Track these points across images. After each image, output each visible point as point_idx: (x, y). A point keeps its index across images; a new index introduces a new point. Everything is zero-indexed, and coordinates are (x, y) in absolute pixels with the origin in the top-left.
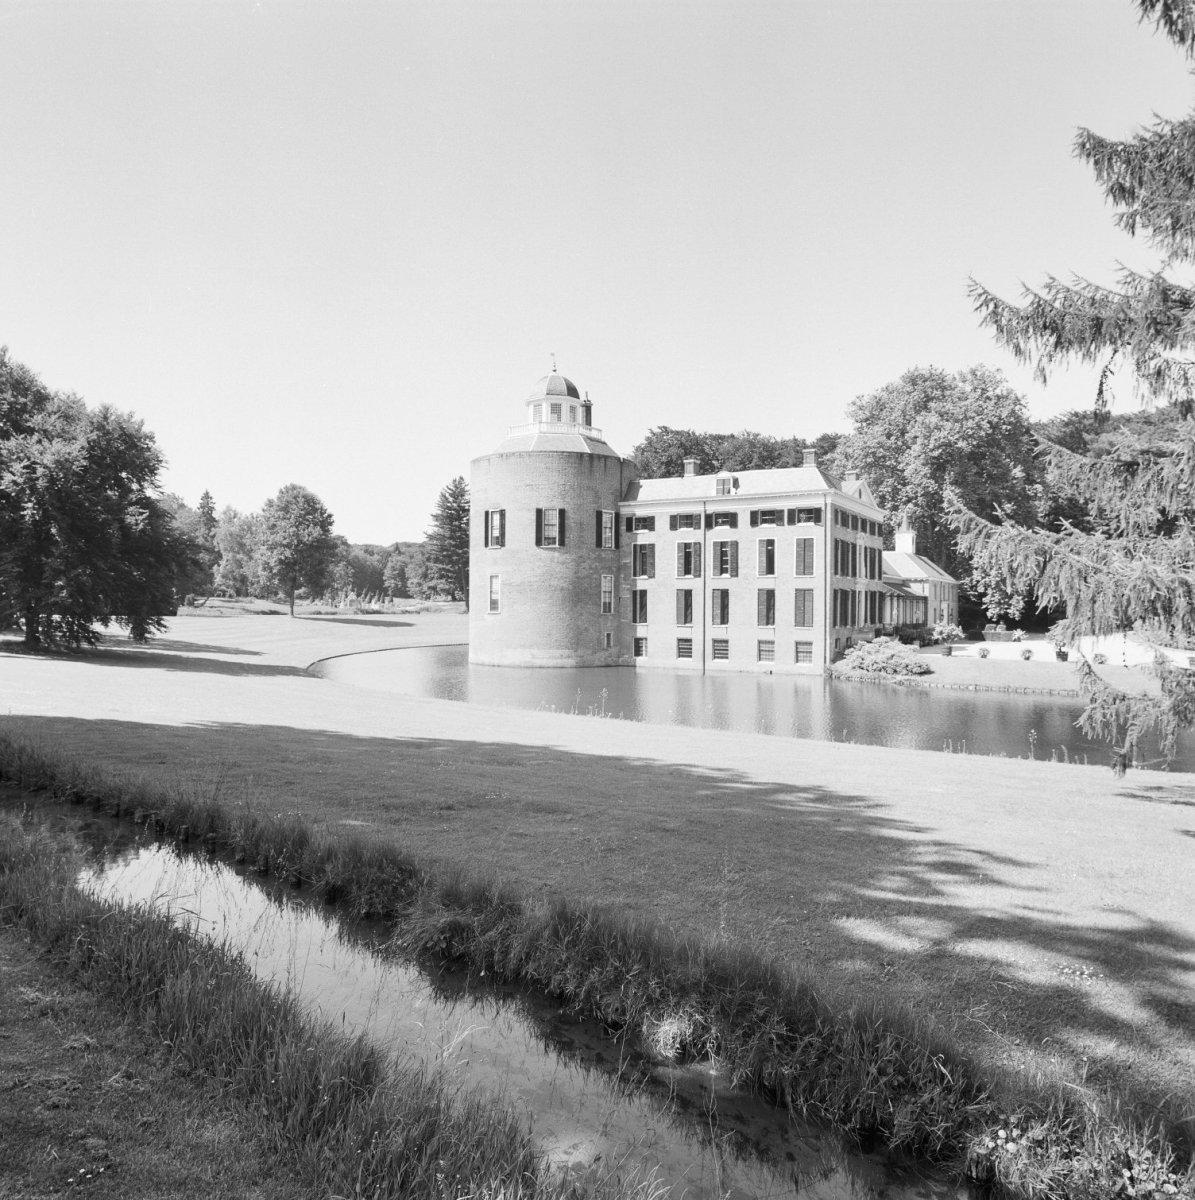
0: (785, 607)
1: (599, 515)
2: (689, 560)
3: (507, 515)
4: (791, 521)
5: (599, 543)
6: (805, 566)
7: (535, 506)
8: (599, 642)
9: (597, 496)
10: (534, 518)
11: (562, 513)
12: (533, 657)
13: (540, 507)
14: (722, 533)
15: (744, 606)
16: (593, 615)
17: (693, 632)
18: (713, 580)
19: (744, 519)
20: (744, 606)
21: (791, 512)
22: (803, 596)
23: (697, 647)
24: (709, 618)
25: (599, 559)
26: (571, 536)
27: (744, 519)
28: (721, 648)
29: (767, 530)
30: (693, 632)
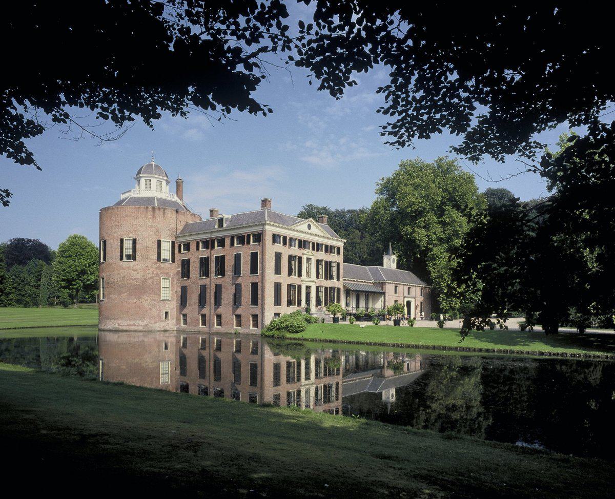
1: (159, 243)
5: (159, 258)
7: (120, 237)
8: (159, 316)
9: (157, 231)
11: (134, 241)
12: (119, 325)
14: (218, 251)
15: (228, 295)
16: (155, 300)
17: (205, 311)
20: (228, 295)
25: (159, 268)
26: (138, 253)
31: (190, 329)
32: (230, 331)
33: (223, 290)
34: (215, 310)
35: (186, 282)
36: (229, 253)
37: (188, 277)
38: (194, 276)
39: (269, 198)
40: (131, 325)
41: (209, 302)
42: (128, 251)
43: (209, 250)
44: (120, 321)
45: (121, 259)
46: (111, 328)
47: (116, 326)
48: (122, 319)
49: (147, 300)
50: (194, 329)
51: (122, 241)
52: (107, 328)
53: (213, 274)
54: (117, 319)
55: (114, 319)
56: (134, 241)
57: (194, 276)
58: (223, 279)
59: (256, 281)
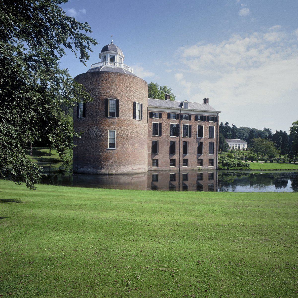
0: (206, 149)
2: (175, 131)
3: (120, 102)
4: (208, 120)
6: (211, 135)
10: (133, 106)
12: (132, 169)
13: (135, 101)
14: (185, 122)
15: (193, 148)
17: (176, 157)
18: (183, 138)
19: (193, 118)
20: (193, 148)
21: (208, 117)
22: (211, 144)
23: (177, 162)
28: (186, 162)
29: (200, 123)
30: (176, 157)
32: (195, 169)
33: (189, 145)
34: (183, 156)
35: (156, 138)
36: (195, 125)
37: (160, 135)
39: (207, 98)
40: (139, 169)
43: (178, 121)
44: (133, 166)
45: (107, 115)
46: (126, 172)
48: (134, 164)
49: (145, 150)
50: (165, 169)
51: (135, 104)
53: (182, 135)
55: (128, 164)
56: (142, 105)
58: (190, 138)
59: (213, 141)
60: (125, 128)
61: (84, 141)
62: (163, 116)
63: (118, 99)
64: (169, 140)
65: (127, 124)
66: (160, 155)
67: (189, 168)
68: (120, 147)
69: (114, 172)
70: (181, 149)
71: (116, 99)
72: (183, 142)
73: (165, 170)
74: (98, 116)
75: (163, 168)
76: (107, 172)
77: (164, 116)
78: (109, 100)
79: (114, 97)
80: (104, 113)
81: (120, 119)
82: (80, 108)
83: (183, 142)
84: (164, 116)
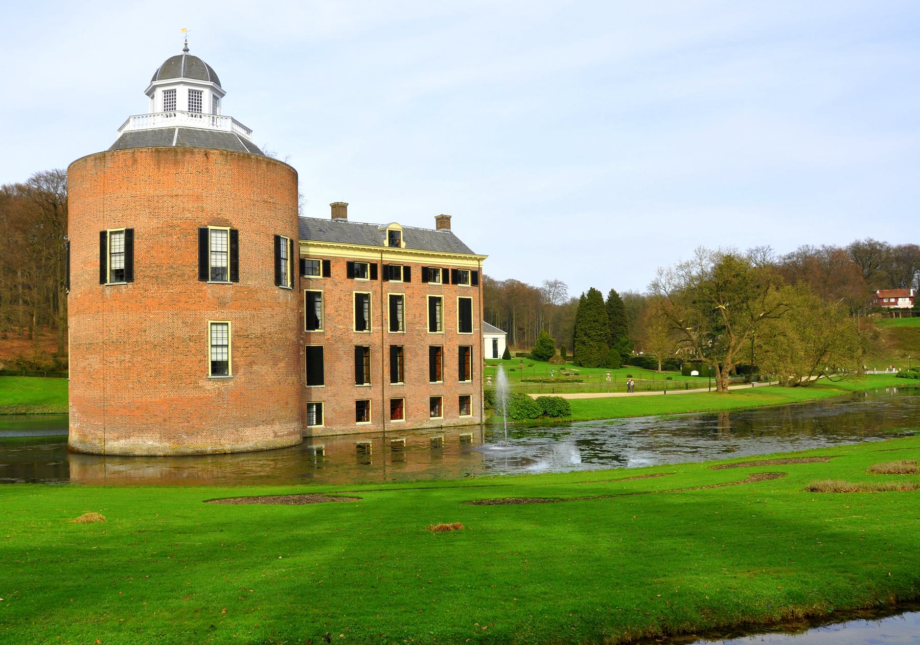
3: (240, 237)
7: (272, 232)
10: (272, 246)
12: (276, 436)
13: (277, 233)
14: (395, 286)
19: (416, 275)
24: (387, 376)
27: (416, 275)
31: (334, 431)
32: (425, 426)
38: (339, 326)
39: (446, 213)
41: (380, 380)
42: (219, 260)
44: (277, 427)
46: (260, 446)
47: (271, 437)
52: (241, 446)
54: (271, 422)
55: (266, 422)
57: (339, 326)
60: (254, 312)
61: (128, 357)
62: (333, 270)
63: (236, 227)
64: (351, 341)
65: (258, 300)
66: (329, 388)
67: (409, 423)
68: (241, 371)
69: (228, 447)
70: (385, 367)
71: (228, 229)
72: (391, 346)
73: (344, 435)
74: (175, 278)
75: (338, 429)
76: (209, 449)
77: (338, 271)
78: (210, 230)
79: (225, 223)
80: (197, 270)
81: (241, 287)
82: (113, 252)
83: (391, 346)
84: (338, 271)
